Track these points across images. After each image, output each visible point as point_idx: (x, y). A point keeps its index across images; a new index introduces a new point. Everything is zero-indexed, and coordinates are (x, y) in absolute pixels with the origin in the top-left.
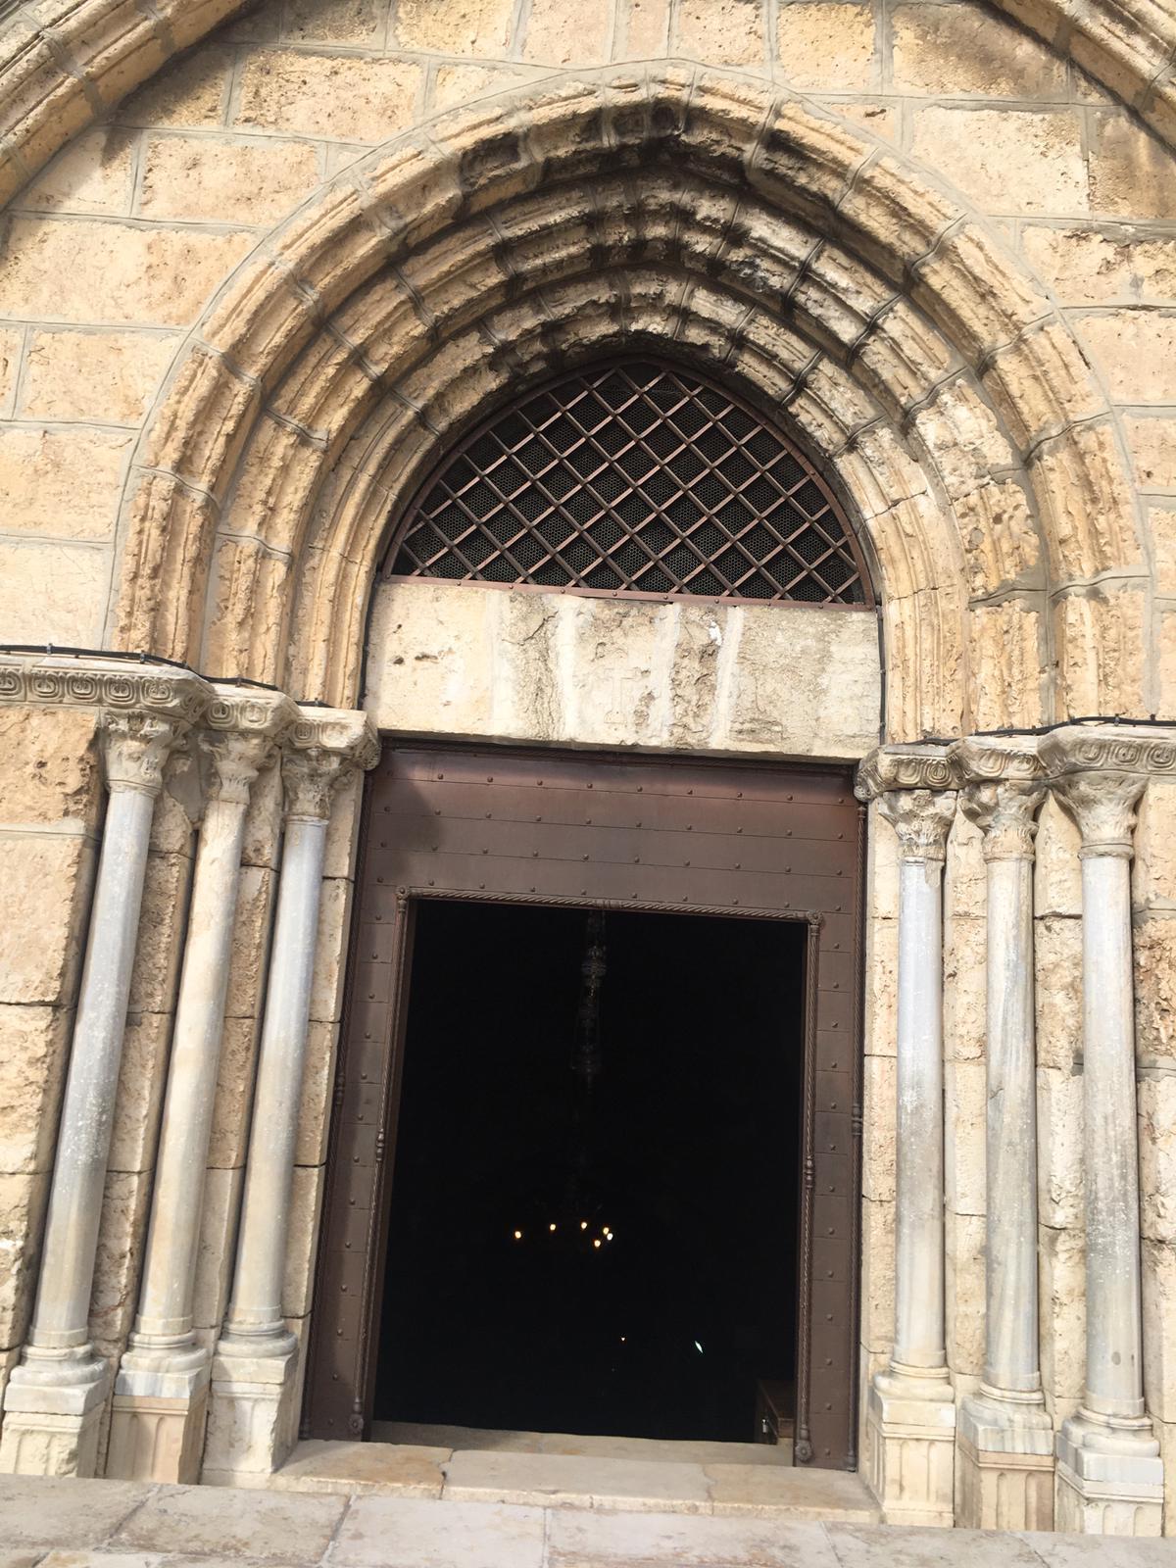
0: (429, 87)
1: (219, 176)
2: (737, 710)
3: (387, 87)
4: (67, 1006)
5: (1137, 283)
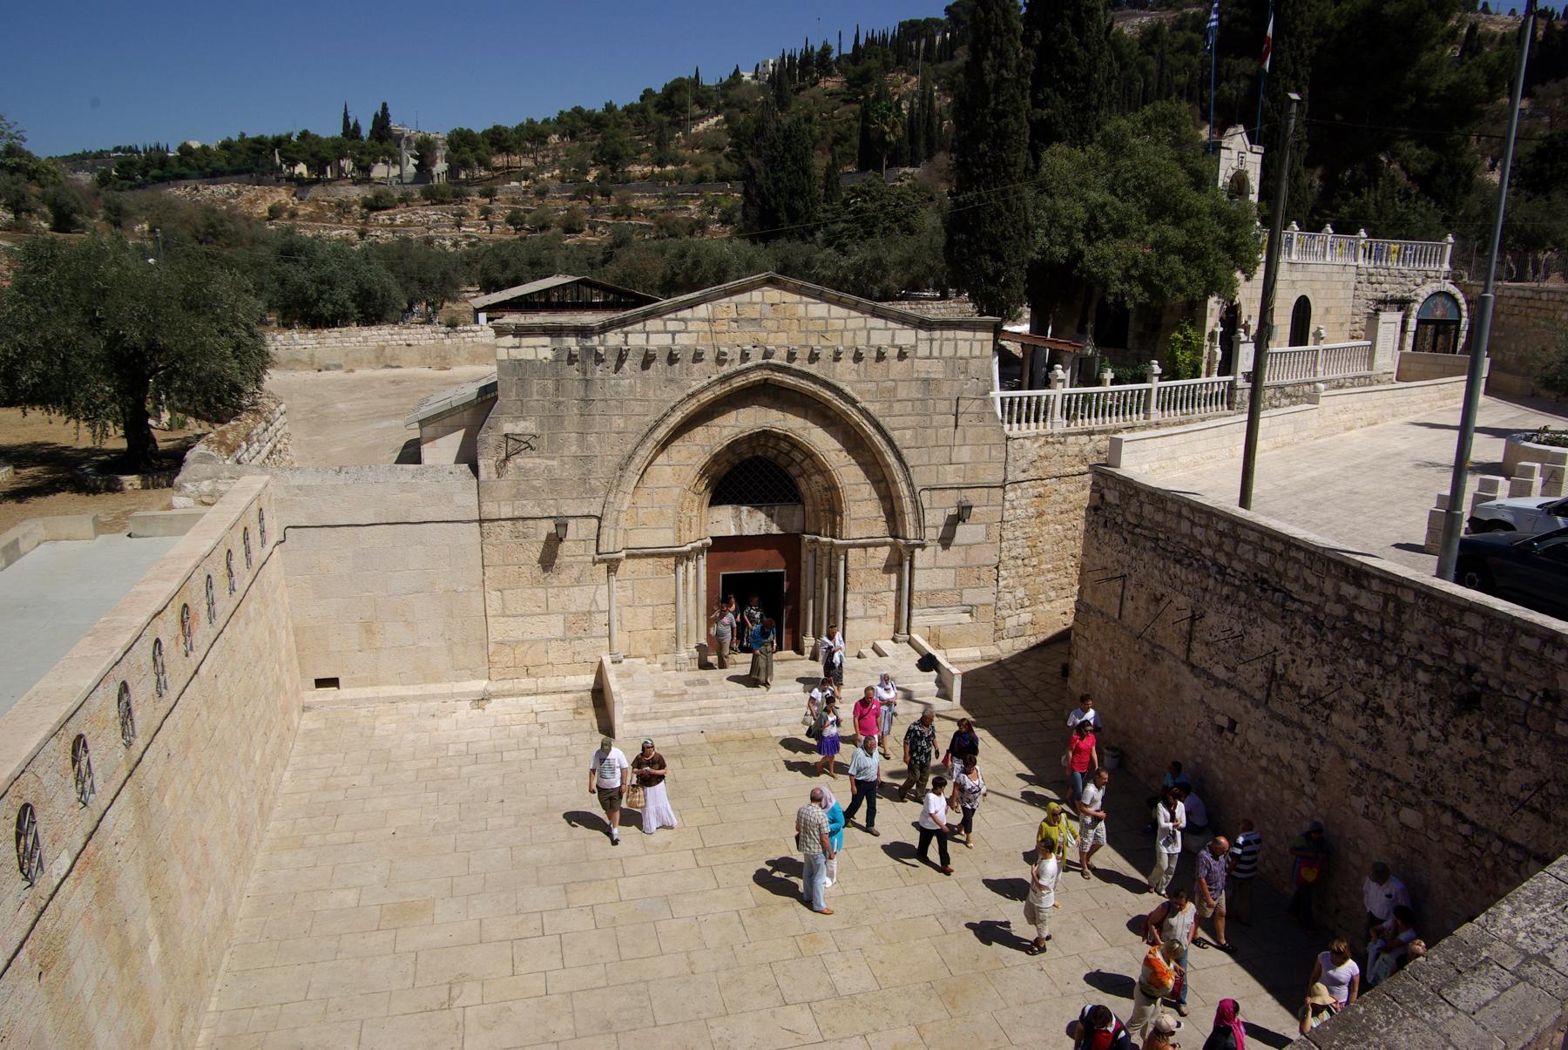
1: (684, 453)
4: (675, 603)
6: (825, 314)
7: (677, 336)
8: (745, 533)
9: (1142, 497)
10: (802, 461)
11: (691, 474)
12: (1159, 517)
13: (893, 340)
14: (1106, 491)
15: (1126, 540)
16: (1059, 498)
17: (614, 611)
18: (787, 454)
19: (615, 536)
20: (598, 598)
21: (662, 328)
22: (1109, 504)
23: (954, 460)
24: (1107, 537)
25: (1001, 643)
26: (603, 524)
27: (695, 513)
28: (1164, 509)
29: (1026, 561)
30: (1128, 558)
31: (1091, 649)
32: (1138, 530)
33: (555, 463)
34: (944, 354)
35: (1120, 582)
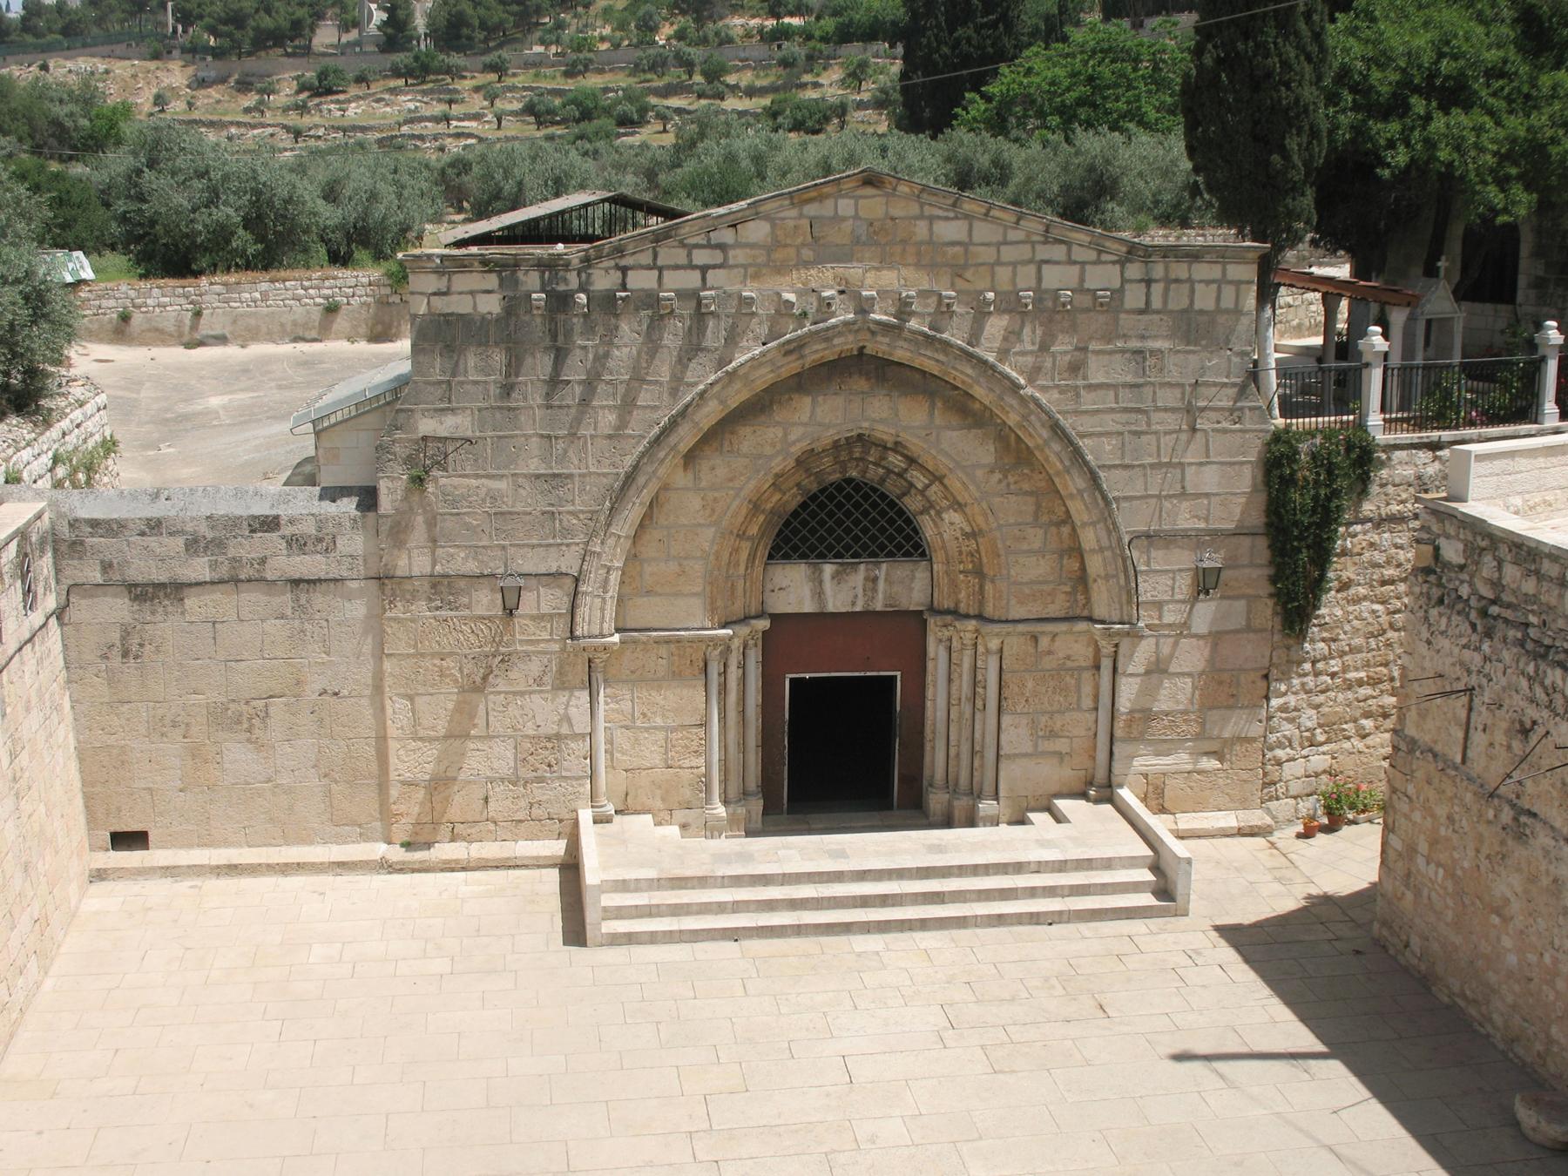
0: (785, 435)
2: (885, 599)
3: (772, 435)
5: (1008, 485)
6: (963, 237)
7: (710, 274)
8: (831, 608)
9: (1503, 550)
10: (927, 486)
11: (735, 507)
12: (1529, 586)
13: (1082, 280)
14: (1442, 542)
15: (1473, 626)
16: (1379, 558)
17: (601, 737)
18: (900, 475)
19: (603, 610)
20: (573, 711)
21: (683, 260)
22: (1447, 565)
23: (1190, 490)
24: (1444, 621)
25: (1273, 805)
26: (583, 588)
27: (742, 570)
28: (1537, 572)
29: (1320, 666)
30: (1477, 658)
31: (1417, 816)
32: (1494, 610)
33: (502, 485)
34: (1171, 306)
35: (1465, 699)
